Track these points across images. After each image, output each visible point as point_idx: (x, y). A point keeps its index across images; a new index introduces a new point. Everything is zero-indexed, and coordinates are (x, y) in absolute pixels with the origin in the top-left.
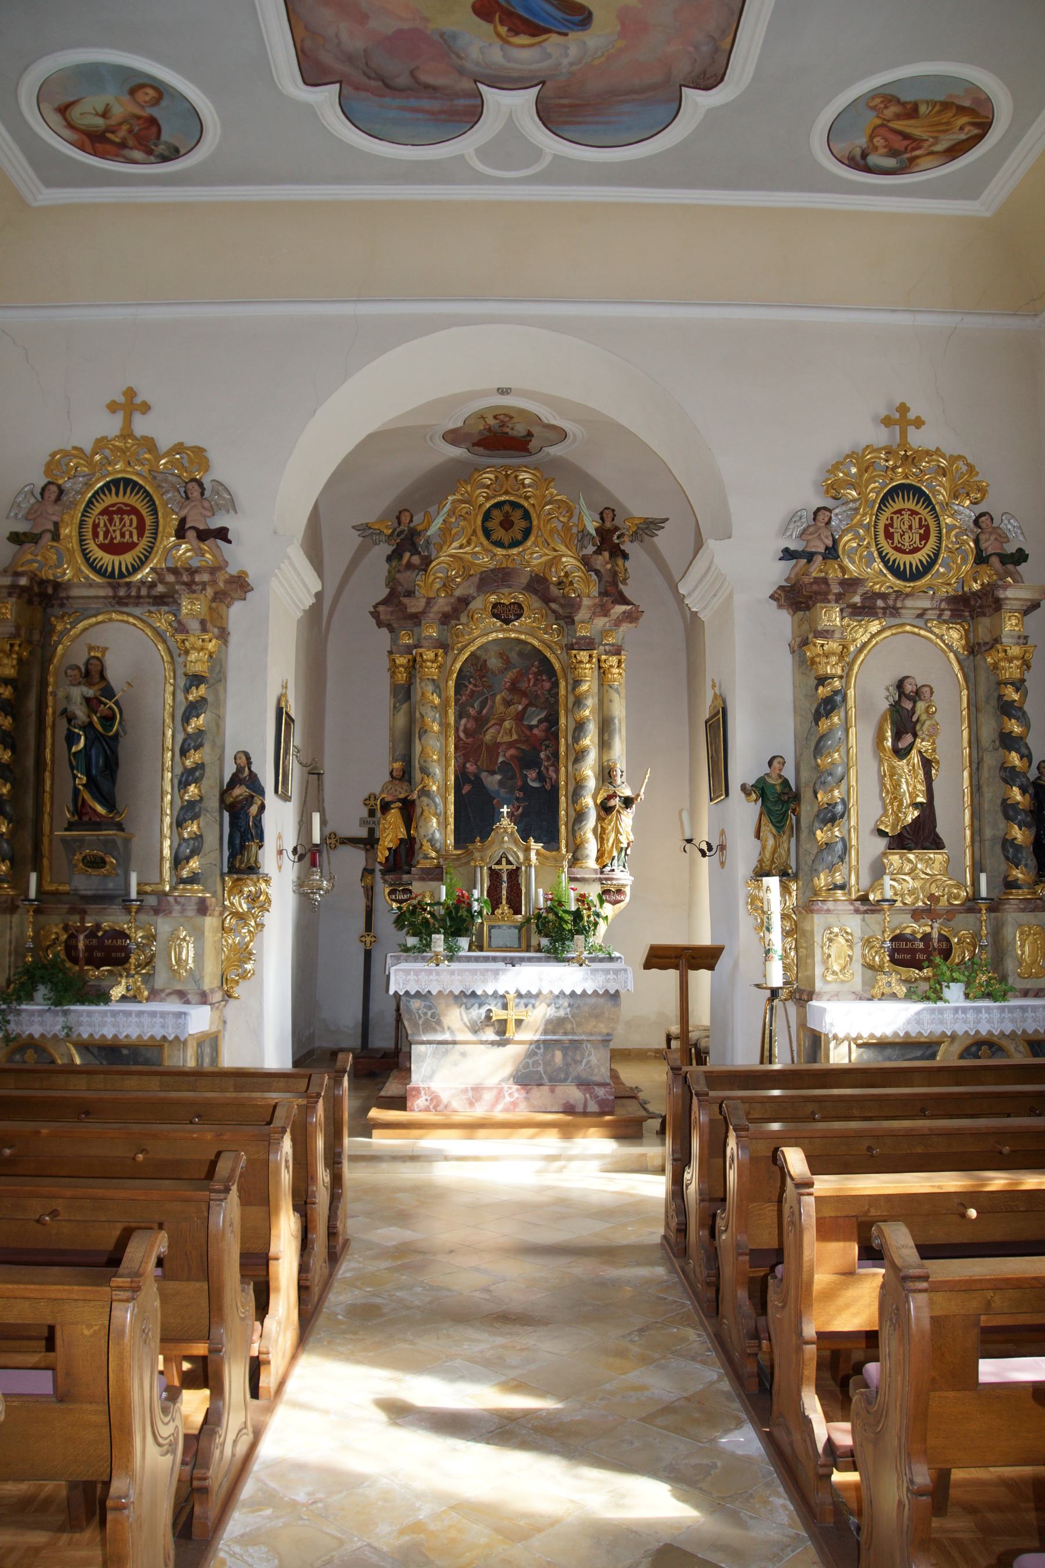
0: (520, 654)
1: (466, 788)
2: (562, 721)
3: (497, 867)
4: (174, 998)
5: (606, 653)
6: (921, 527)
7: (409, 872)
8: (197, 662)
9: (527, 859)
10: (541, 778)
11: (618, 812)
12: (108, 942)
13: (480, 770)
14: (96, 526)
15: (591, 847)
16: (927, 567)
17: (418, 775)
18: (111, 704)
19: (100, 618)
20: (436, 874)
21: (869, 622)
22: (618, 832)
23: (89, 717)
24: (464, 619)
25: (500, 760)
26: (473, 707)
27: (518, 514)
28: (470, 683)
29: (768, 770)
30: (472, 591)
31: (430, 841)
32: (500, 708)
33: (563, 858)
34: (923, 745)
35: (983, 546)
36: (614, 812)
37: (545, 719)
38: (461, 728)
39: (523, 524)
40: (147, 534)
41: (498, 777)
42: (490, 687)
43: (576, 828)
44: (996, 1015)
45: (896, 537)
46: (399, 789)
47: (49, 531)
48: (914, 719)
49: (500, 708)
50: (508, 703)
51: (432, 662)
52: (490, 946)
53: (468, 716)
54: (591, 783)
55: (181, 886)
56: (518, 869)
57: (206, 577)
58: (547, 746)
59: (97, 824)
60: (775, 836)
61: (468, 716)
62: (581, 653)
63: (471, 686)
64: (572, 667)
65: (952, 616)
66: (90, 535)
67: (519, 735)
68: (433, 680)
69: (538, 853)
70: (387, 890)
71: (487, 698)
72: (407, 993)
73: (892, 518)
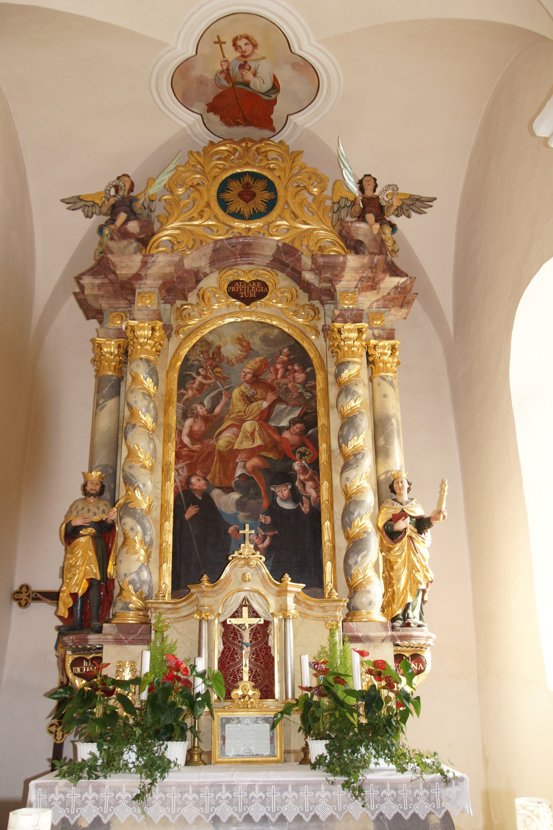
0: (265, 339)
1: (191, 512)
3: (234, 621)
7: (99, 631)
10: (295, 496)
11: (410, 538)
13: (210, 486)
17: (122, 491)
22: (412, 568)
24: (192, 298)
25: (239, 472)
26: (202, 403)
27: (260, 185)
28: (199, 374)
30: (203, 264)
32: (238, 405)
36: (405, 539)
37: (299, 419)
38: (186, 431)
39: (267, 195)
41: (236, 496)
42: (224, 379)
43: (351, 561)
46: (94, 509)
49: (238, 405)
50: (248, 399)
53: (196, 416)
56: (267, 623)
58: (303, 455)
61: (196, 416)
62: (348, 326)
63: (199, 379)
67: (263, 440)
69: (297, 601)
71: (220, 393)
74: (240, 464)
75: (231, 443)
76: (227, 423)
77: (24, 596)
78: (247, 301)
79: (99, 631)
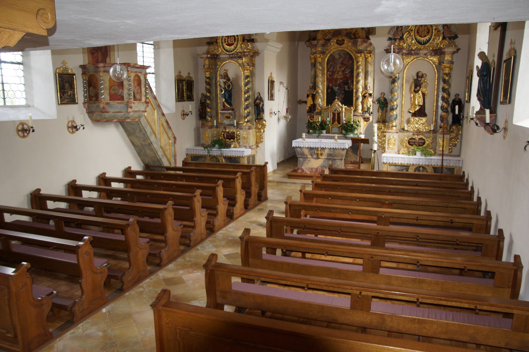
0: (344, 54)
1: (329, 91)
2: (355, 72)
4: (244, 147)
5: (367, 53)
6: (427, 30)
7: (313, 113)
8: (247, 73)
9: (342, 110)
10: (349, 88)
12: (231, 135)
14: (225, 40)
15: (360, 107)
16: (428, 41)
18: (229, 83)
19: (227, 61)
20: (320, 113)
21: (411, 56)
23: (225, 86)
24: (329, 45)
25: (338, 83)
29: (381, 96)
31: (319, 105)
32: (338, 69)
33: (352, 110)
34: (423, 89)
35: (445, 34)
36: (366, 98)
38: (328, 74)
40: (236, 41)
41: (337, 87)
44: (424, 160)
45: (420, 33)
47: (215, 41)
48: (421, 83)
49: (338, 69)
50: (340, 68)
51: (319, 57)
52: (331, 132)
53: (330, 71)
54: (361, 90)
55: (245, 123)
57: (247, 54)
58: (350, 79)
59: (229, 110)
60: (381, 113)
63: (331, 63)
64: (357, 58)
65: (434, 54)
66: (224, 42)
68: (320, 62)
69: (345, 108)
70: (309, 117)
71: (335, 67)
72: (296, 147)
73: (419, 28)
74: (338, 81)
75: (337, 77)
76: (336, 73)
77: (300, 102)
78: (340, 45)
79: (313, 113)
